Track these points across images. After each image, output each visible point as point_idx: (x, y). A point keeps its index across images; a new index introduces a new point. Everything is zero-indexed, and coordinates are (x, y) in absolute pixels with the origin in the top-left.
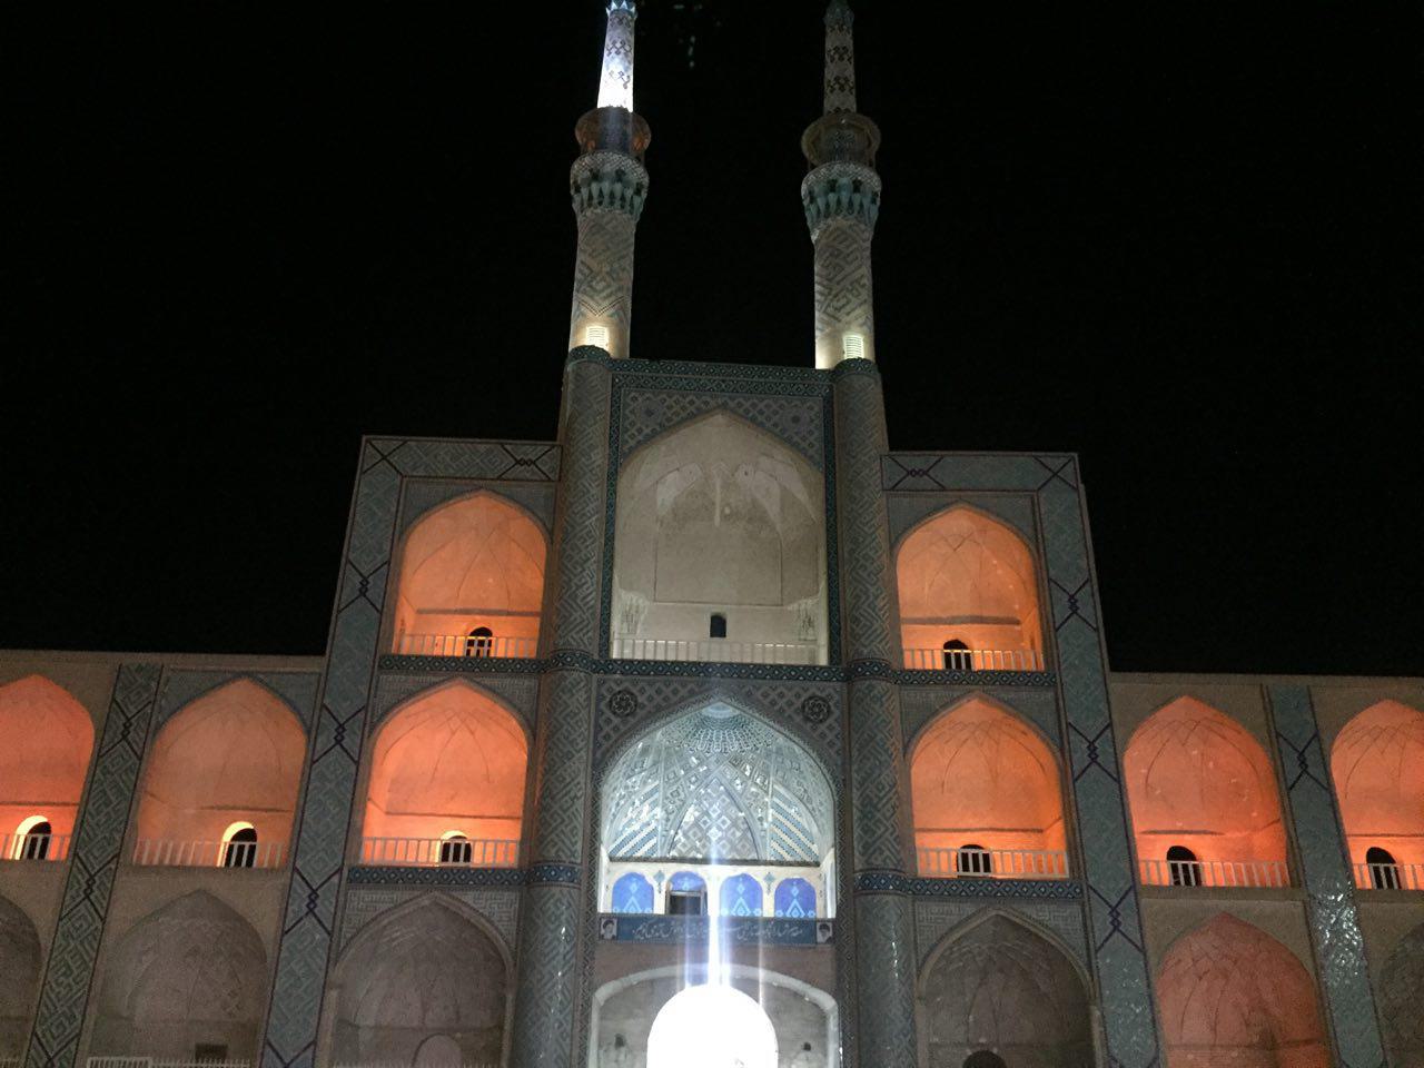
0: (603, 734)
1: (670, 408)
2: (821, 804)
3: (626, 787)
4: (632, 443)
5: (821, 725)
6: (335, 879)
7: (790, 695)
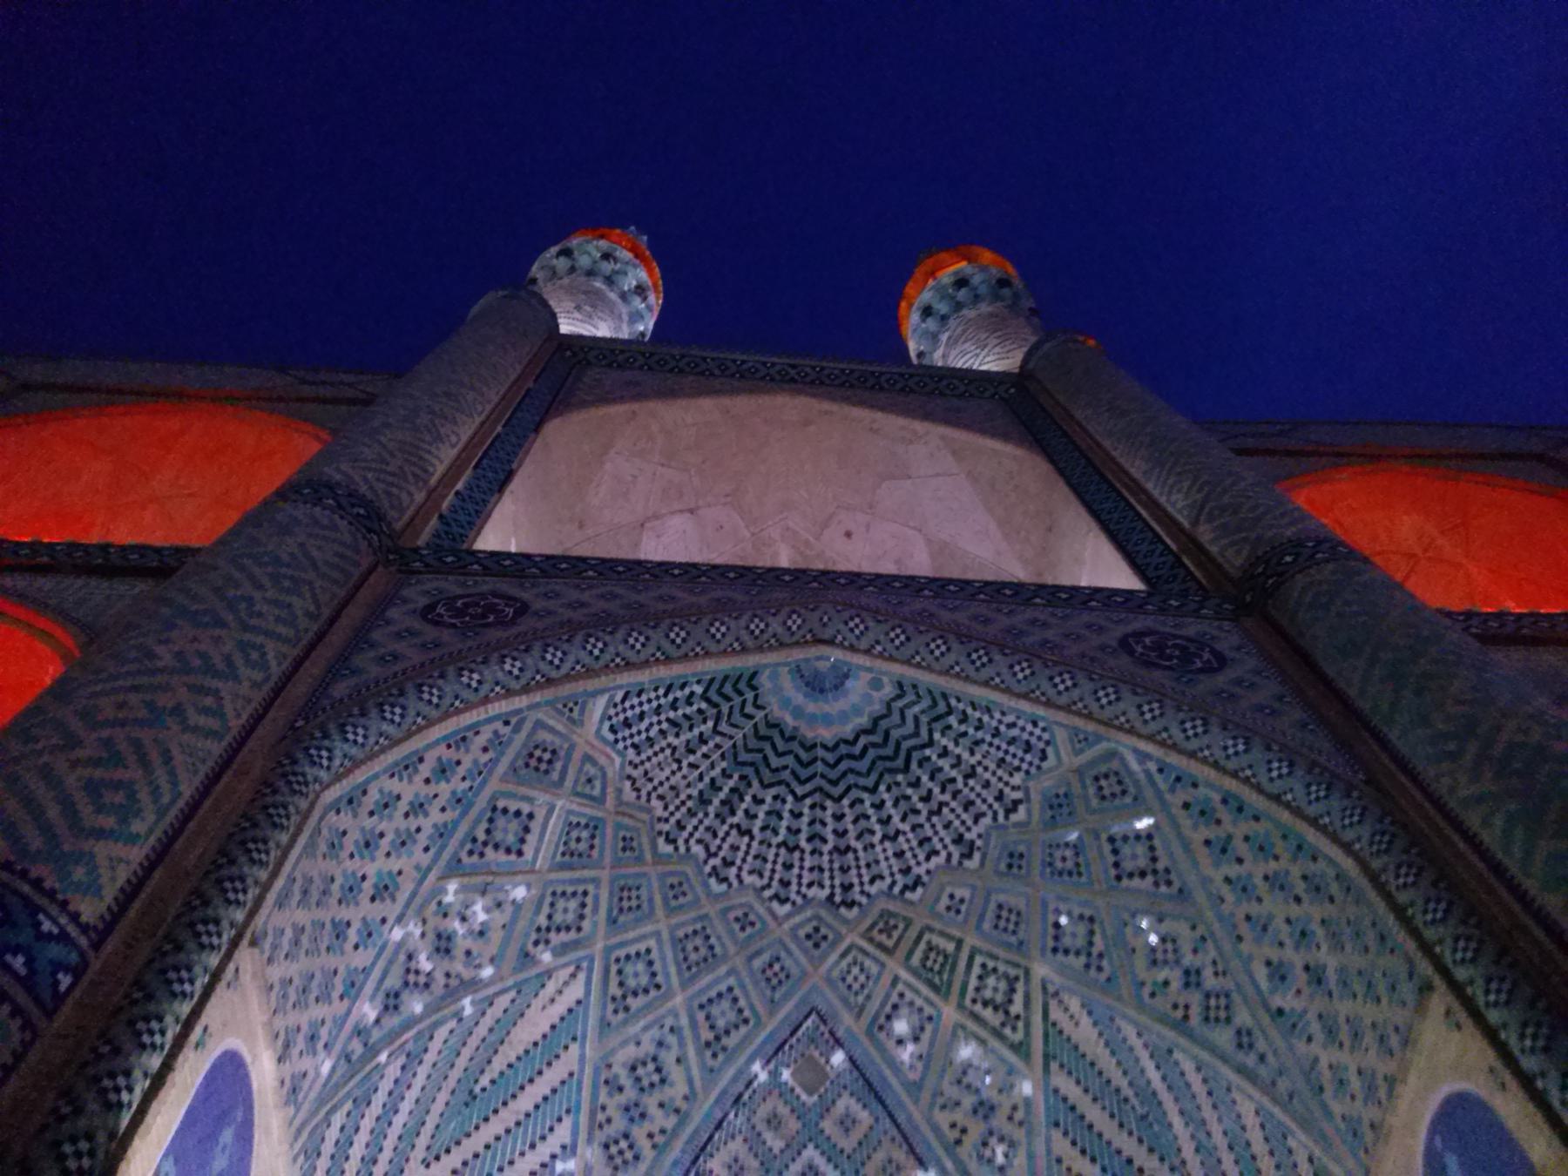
2: (1279, 974)
3: (443, 945)
5: (1202, 677)
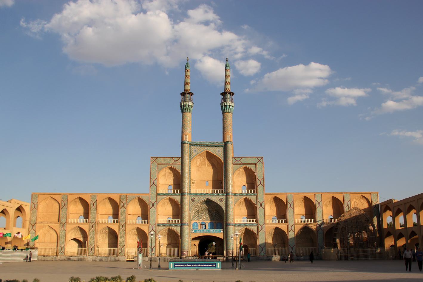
0: (190, 205)
1: (199, 150)
4: (193, 156)
6: (155, 225)
7: (218, 198)
